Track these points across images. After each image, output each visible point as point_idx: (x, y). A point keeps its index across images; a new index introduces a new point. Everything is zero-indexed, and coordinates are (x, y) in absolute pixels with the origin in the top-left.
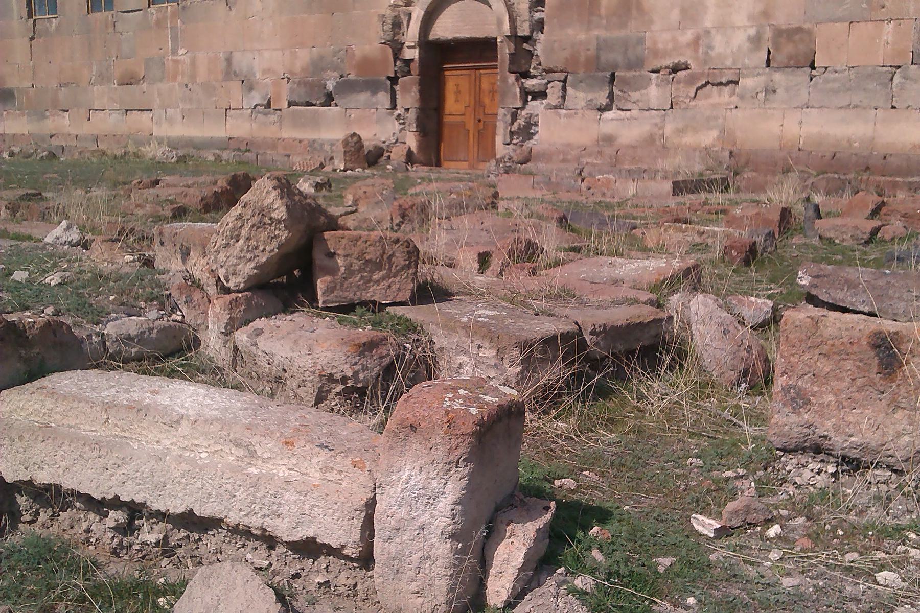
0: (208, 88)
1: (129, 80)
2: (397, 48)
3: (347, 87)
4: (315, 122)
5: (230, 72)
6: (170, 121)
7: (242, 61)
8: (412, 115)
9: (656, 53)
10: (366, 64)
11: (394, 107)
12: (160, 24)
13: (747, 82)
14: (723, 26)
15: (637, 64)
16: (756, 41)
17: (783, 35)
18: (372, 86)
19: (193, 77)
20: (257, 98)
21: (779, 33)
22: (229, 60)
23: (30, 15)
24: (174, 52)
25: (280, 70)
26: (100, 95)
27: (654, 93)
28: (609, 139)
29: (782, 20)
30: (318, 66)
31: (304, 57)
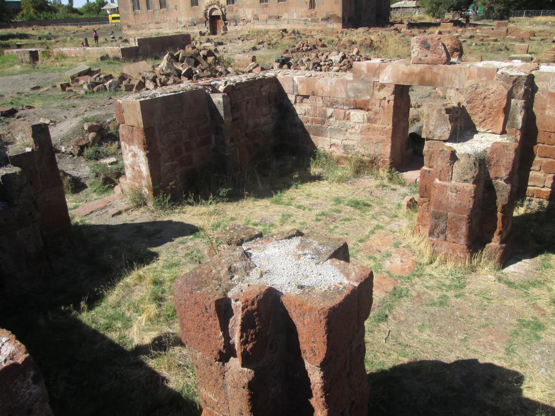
0: (173, 24)
1: (157, 23)
2: (206, 17)
3: (198, 23)
4: (193, 29)
5: (177, 21)
6: (166, 30)
7: (179, 19)
8: (209, 27)
9: (241, 18)
10: (201, 19)
11: (206, 26)
12: (163, 12)
13: (252, 22)
14: (248, 14)
15: (239, 19)
16: (252, 16)
17: (255, 15)
18: (202, 23)
19: (170, 22)
20: (183, 25)
21: (254, 15)
22: (177, 19)
23: (134, 10)
24: (166, 18)
25: (186, 21)
26: (152, 26)
27: (241, 23)
28: (237, 30)
29: (255, 13)
30: (193, 20)
31: (190, 19)
